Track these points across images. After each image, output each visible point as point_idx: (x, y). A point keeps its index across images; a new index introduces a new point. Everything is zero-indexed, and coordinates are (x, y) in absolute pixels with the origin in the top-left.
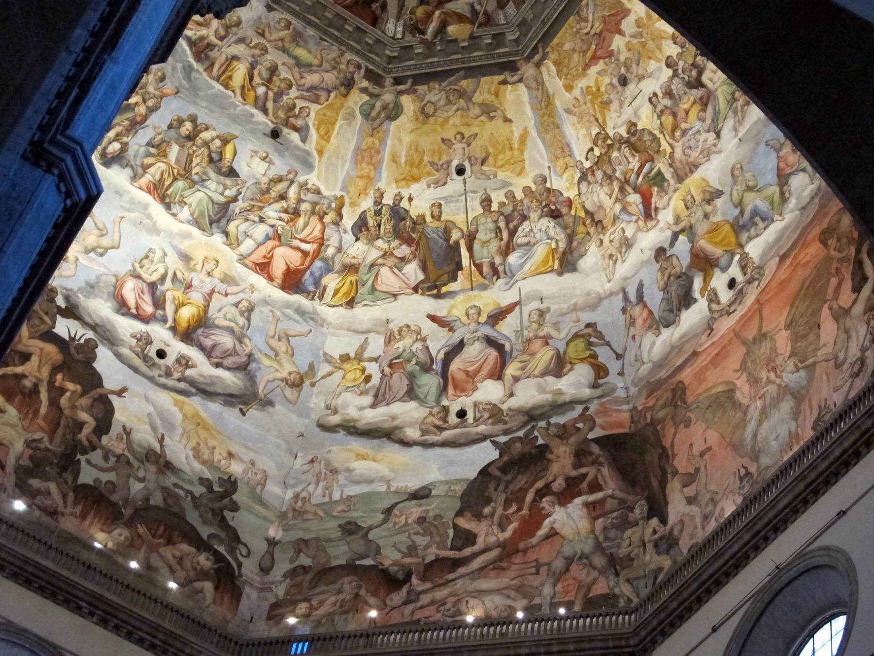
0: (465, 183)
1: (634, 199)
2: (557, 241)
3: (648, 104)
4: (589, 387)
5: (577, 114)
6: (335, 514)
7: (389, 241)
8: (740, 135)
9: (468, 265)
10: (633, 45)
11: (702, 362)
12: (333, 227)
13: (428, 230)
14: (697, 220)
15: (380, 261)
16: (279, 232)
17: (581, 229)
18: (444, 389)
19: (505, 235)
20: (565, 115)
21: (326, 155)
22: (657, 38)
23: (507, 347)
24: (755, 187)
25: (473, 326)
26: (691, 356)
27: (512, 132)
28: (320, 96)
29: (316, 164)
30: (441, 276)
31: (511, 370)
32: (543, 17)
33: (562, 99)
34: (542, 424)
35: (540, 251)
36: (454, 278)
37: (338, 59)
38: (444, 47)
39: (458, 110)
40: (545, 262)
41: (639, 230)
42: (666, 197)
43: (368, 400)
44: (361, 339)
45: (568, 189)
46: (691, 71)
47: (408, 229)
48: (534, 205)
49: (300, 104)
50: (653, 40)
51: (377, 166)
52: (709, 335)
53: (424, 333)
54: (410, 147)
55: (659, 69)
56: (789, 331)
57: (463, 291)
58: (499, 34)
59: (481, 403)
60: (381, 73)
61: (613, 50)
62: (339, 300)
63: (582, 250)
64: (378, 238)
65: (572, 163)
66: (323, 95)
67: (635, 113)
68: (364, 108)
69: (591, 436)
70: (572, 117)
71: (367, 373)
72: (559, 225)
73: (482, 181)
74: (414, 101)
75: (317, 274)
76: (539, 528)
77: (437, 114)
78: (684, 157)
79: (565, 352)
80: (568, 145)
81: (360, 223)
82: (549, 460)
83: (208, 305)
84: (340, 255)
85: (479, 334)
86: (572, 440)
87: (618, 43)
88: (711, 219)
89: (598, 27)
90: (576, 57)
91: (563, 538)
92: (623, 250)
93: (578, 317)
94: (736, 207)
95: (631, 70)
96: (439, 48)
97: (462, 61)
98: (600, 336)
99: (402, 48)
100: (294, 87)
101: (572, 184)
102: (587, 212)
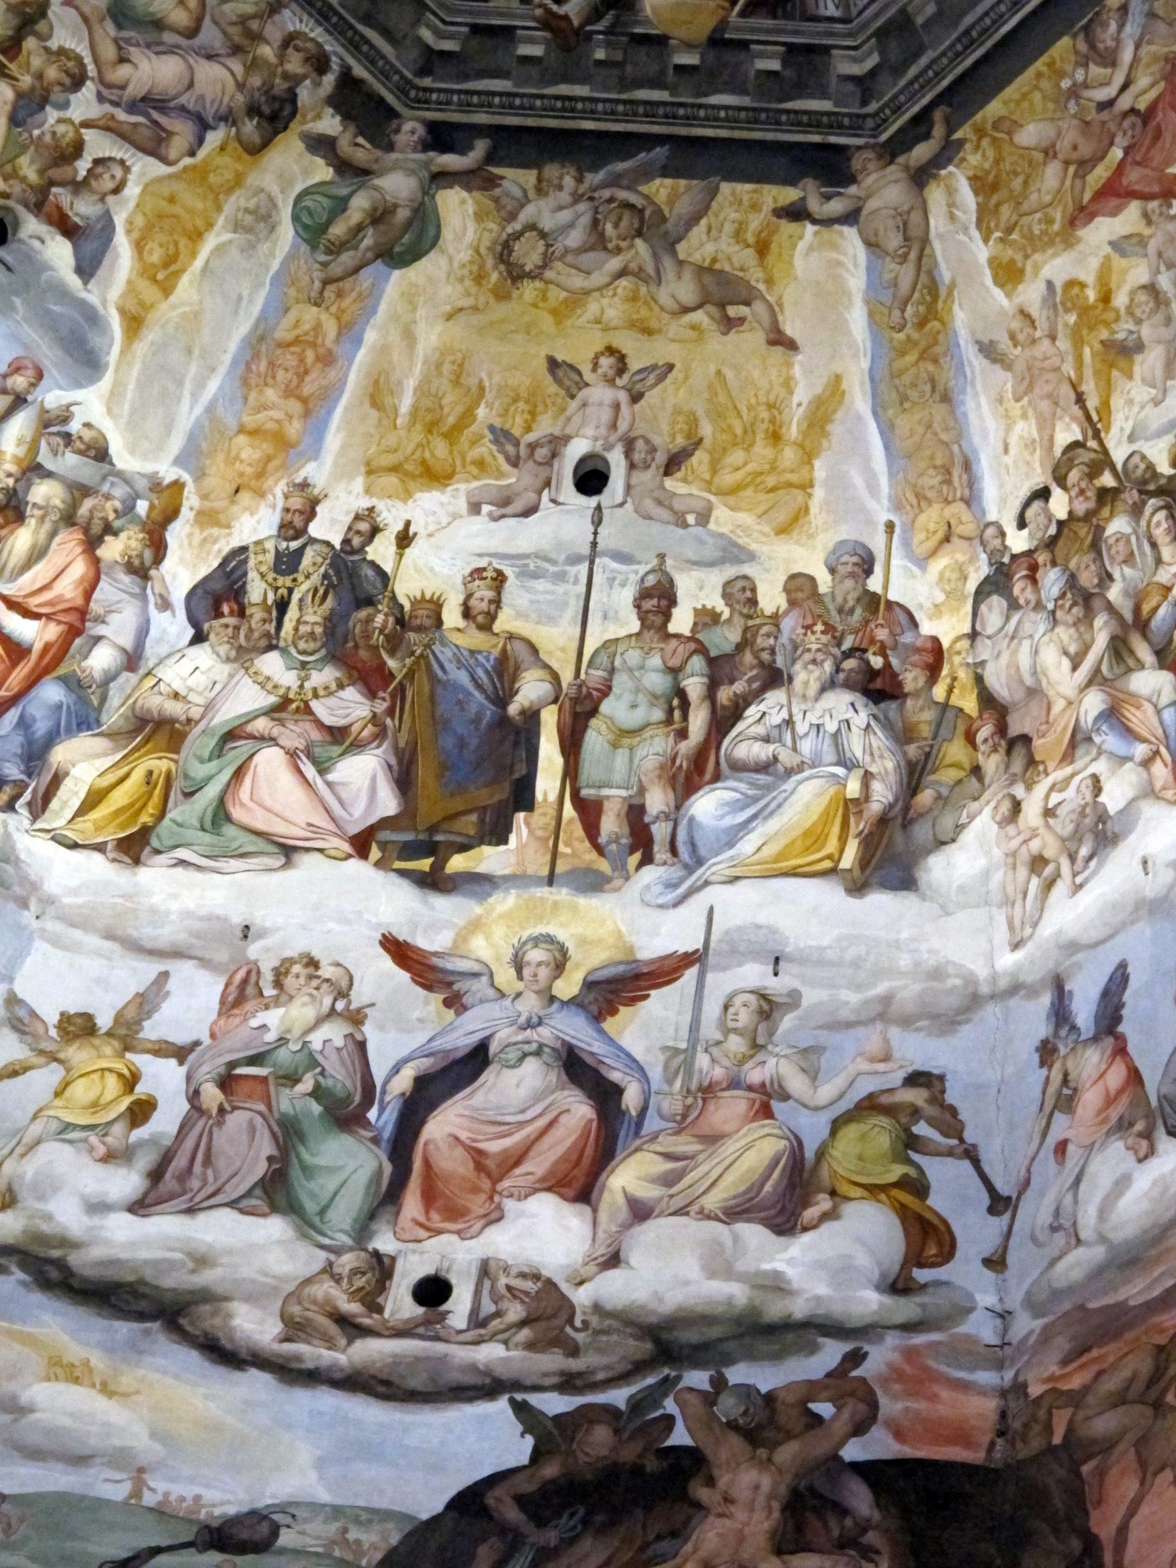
0: (598, 518)
2: (867, 777)
4: (878, 1288)
5: (1020, 366)
7: (304, 665)
9: (553, 796)
12: (126, 579)
13: (445, 654)
15: (261, 725)
17: (956, 751)
19: (698, 721)
21: (150, 336)
23: (631, 1099)
25: (530, 1004)
27: (788, 385)
28: (170, 134)
29: (113, 357)
30: (458, 815)
32: (968, 20)
34: (698, 1379)
36: (498, 834)
37: (254, 25)
38: (619, 56)
39: (622, 273)
40: (813, 837)
41: (1150, 792)
44: (149, 970)
45: (937, 611)
47: (378, 639)
48: (816, 640)
49: (98, 145)
53: (359, 996)
54: (439, 366)
57: (517, 880)
58: (809, 49)
59: (506, 1269)
60: (390, 98)
62: (98, 829)
63: (946, 822)
64: (271, 648)
65: (969, 528)
66: (182, 131)
68: (308, 203)
69: (852, 1452)
70: (999, 375)
71: (141, 1089)
72: (888, 725)
73: (655, 527)
74: (479, 217)
75: (41, 728)
77: (549, 274)
79: (821, 1154)
80: (967, 466)
81: (218, 585)
82: (698, 1506)
84: (133, 678)
85: (544, 1034)
86: (787, 1453)
90: (1051, 176)
93: (887, 1041)
96: (600, 54)
97: (670, 113)
98: (950, 1122)
99: (476, 29)
100: (89, 90)
102: (987, 699)
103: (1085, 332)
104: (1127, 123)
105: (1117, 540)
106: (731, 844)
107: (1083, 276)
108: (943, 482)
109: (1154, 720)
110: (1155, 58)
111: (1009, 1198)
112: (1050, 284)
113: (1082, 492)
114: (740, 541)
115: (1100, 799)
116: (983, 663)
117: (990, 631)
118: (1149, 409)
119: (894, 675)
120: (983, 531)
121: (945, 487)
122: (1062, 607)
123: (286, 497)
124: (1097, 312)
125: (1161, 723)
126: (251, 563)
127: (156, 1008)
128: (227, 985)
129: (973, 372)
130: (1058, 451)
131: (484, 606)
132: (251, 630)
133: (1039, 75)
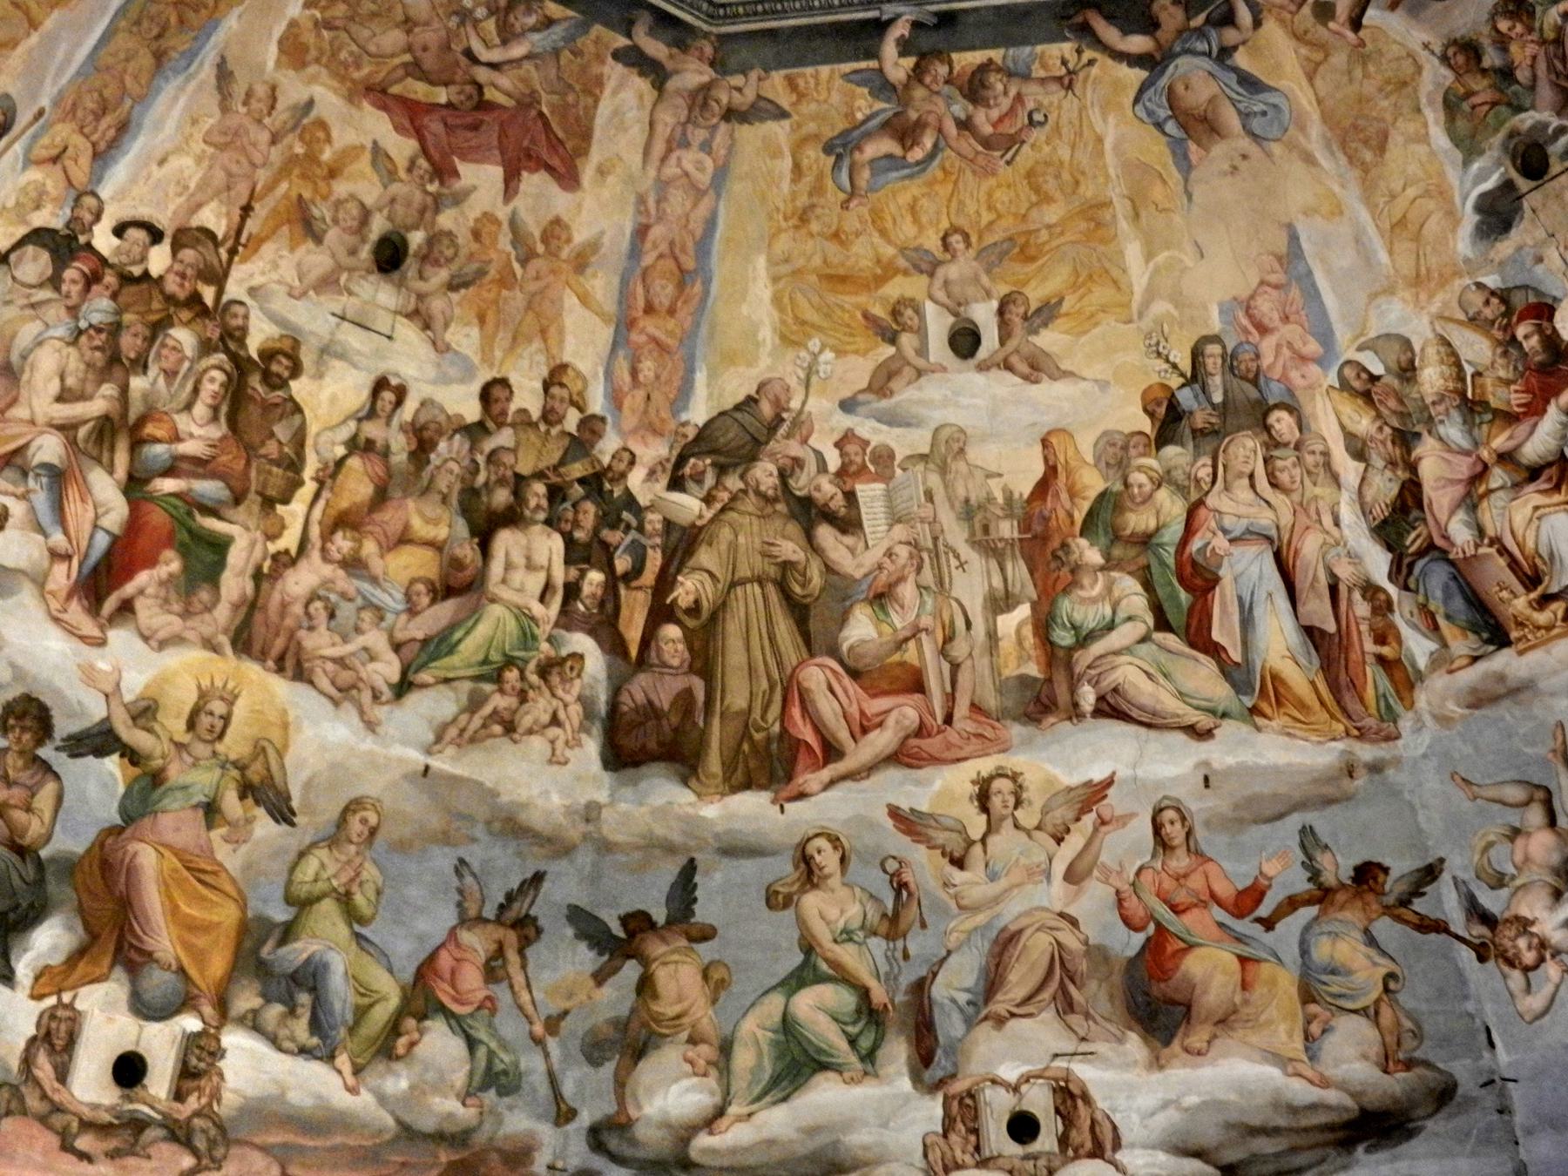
5: (232, 121)
8: (436, 763)
10: (495, 240)
14: (185, 788)
20: (206, 70)
22: (538, 315)
24: (362, 921)
41: (40, 582)
46: (501, 482)
55: (469, 372)
61: (455, 174)
70: (211, 101)
78: (298, 609)
80: (123, 128)
88: (217, 834)
89: (501, 89)
90: (392, 39)
94: (289, 900)
95: (429, 270)
103: (296, 171)
104: (469, 89)
105: (174, 348)
107: (335, 134)
108: (93, 112)
109: (87, 528)
110: (525, 80)
112: (310, 104)
113: (183, 276)
117: (18, 274)
118: (283, 290)
120: (86, 193)
121: (91, 117)
122: (91, 338)
124: (318, 171)
125: (92, 537)
129: (197, 72)
130: (195, 222)
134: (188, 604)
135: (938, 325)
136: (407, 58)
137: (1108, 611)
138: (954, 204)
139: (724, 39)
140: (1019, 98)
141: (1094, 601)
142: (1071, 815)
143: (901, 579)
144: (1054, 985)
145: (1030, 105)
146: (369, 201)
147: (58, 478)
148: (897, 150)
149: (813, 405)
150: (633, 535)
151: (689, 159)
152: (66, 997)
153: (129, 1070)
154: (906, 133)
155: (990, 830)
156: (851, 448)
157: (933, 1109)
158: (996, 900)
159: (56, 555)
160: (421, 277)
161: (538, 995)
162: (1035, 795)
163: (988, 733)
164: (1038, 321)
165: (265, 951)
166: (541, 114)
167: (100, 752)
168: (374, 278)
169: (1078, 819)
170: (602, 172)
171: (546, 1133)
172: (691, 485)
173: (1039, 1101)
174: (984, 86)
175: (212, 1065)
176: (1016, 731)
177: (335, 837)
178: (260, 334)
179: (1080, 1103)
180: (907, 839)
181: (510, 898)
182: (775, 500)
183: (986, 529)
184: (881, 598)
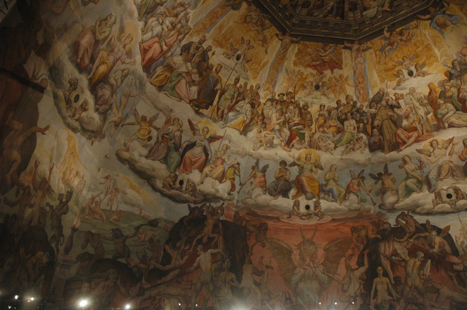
0: (236, 65)
1: (286, 132)
2: (247, 118)
3: (319, 106)
6: (111, 220)
8: (343, 157)
9: (215, 105)
11: (280, 226)
13: (211, 75)
15: (184, 75)
16: (163, 34)
17: (256, 118)
18: (179, 165)
19: (234, 101)
21: (204, 5)
22: (342, 89)
23: (210, 157)
24: (337, 182)
25: (202, 137)
26: (276, 217)
30: (204, 103)
31: (206, 170)
32: (312, 30)
33: (289, 63)
34: (208, 204)
35: (241, 118)
39: (256, 30)
40: (239, 124)
41: (281, 145)
42: (300, 146)
43: (145, 152)
46: (343, 114)
48: (250, 96)
50: (340, 88)
51: (212, 24)
52: (288, 218)
55: (334, 100)
56: (324, 252)
59: (191, 181)
61: (324, 73)
64: (190, 62)
67: (312, 103)
69: (221, 219)
70: (286, 75)
74: (246, 9)
75: (158, 64)
76: (194, 262)
77: (249, 24)
78: (317, 140)
80: (275, 82)
82: (205, 225)
83: (113, 67)
85: (203, 143)
87: (328, 73)
89: (327, 59)
90: (308, 58)
91: (202, 270)
92: (268, 145)
94: (325, 180)
95: (324, 88)
98: (239, 172)
101: (265, 97)
102: (262, 114)
104: (322, 61)
106: (231, 121)
107: (304, 73)
111: (242, 184)
112: (300, 70)
113: (289, 99)
114: (249, 77)
115: (273, 140)
116: (264, 109)
117: (267, 105)
119: (255, 105)
123: (202, 37)
126: (193, 45)
127: (155, 120)
128: (167, 119)
131: (218, 70)
132: (188, 57)
133: (315, 45)
134: (301, 143)
135: (405, 72)
136: (312, 59)
137: (447, 110)
138: (403, 53)
139: (359, 40)
140: (409, 33)
141: (444, 109)
142: (447, 145)
143: (410, 113)
144: (450, 172)
145: (411, 33)
146: (312, 81)
147: (280, 131)
148: (391, 47)
149: (389, 90)
150: (366, 117)
151: (359, 59)
152: (297, 199)
153: (307, 207)
154: (391, 44)
155: (434, 150)
156: (396, 95)
157: (433, 196)
158: (437, 161)
159: (282, 141)
160: (323, 89)
161: (367, 187)
162: (440, 143)
163: (430, 134)
164: (422, 67)
165: (324, 188)
166: (334, 60)
167: (294, 166)
168: (316, 91)
169: (449, 145)
170: (346, 66)
171: (372, 207)
172: (372, 107)
173: (451, 191)
174: (402, 33)
175: (319, 205)
176: (435, 133)
177: (330, 170)
178: (302, 104)
179: (459, 191)
180: (420, 154)
181: (359, 174)
182: (386, 106)
183: (422, 102)
184: (407, 117)
